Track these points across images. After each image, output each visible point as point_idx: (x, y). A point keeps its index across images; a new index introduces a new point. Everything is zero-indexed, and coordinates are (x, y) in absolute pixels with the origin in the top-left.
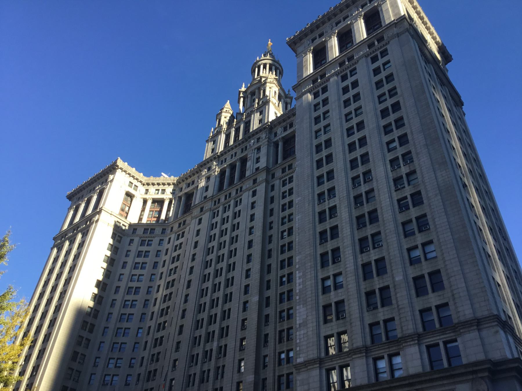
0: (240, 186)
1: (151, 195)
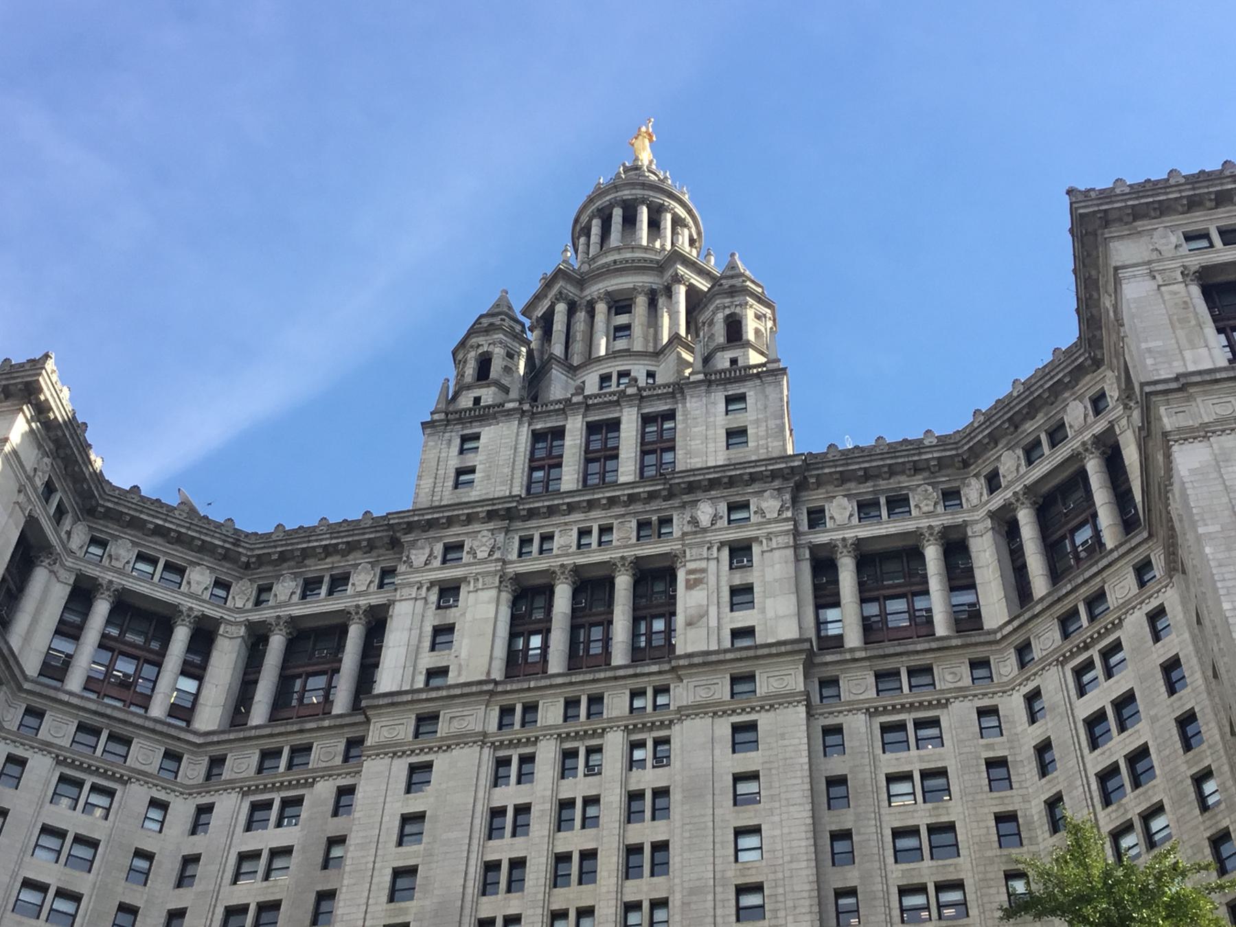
0: (659, 680)
1: (120, 572)
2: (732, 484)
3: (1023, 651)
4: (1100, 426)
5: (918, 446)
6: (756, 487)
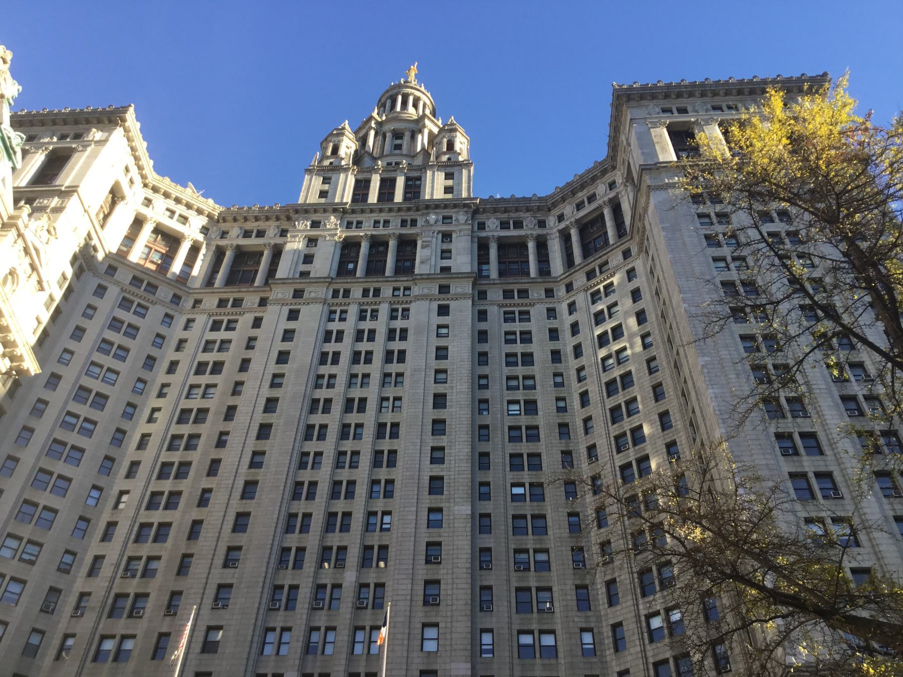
0: (406, 284)
2: (448, 207)
3: (569, 287)
4: (612, 195)
5: (529, 200)
6: (455, 210)
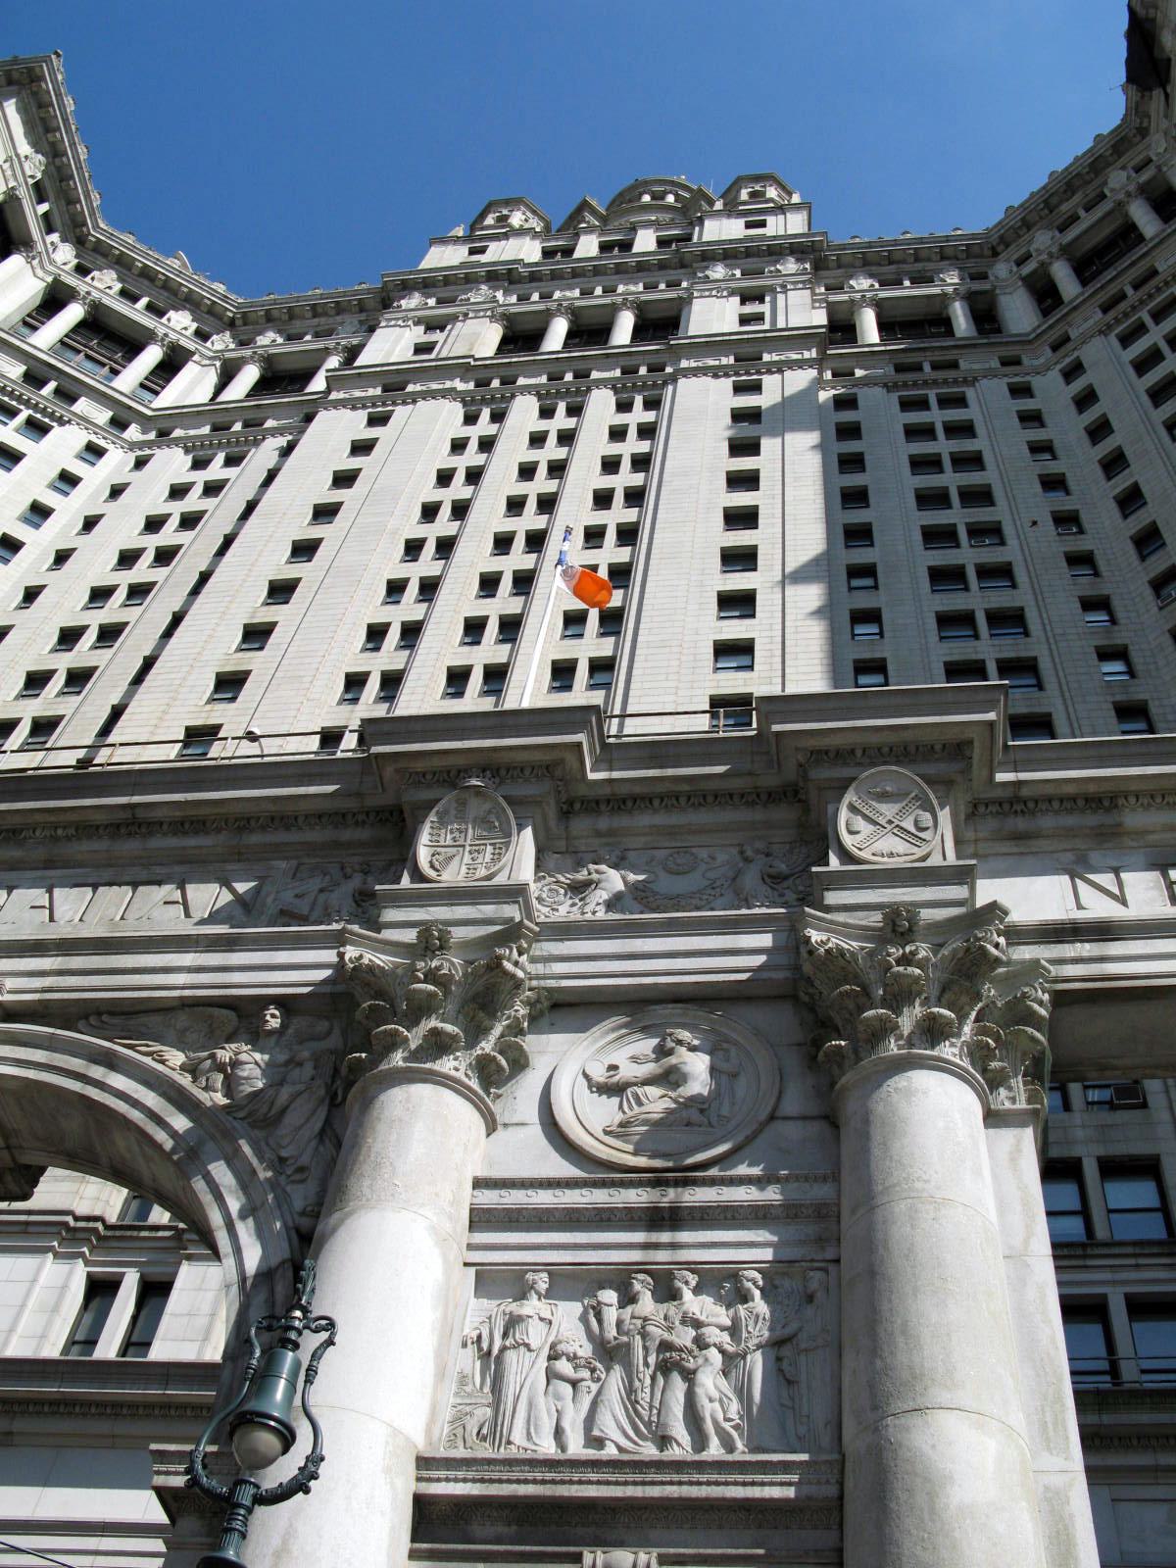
0: (654, 359)
